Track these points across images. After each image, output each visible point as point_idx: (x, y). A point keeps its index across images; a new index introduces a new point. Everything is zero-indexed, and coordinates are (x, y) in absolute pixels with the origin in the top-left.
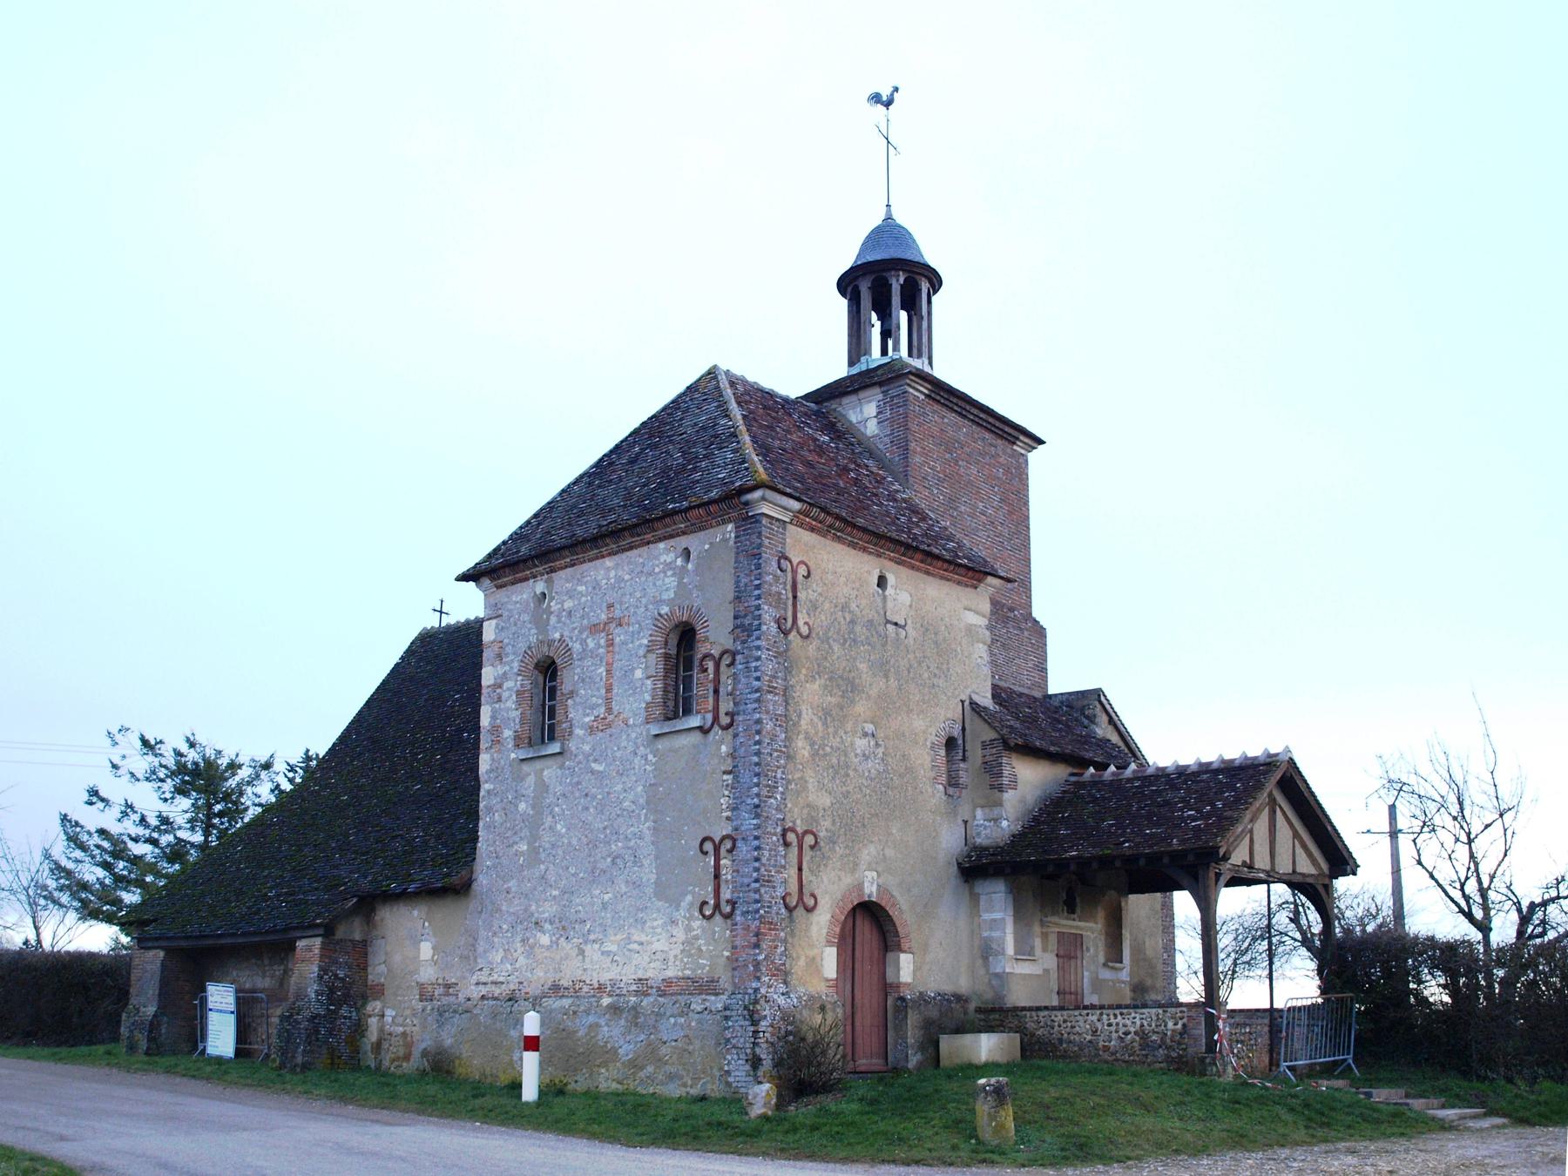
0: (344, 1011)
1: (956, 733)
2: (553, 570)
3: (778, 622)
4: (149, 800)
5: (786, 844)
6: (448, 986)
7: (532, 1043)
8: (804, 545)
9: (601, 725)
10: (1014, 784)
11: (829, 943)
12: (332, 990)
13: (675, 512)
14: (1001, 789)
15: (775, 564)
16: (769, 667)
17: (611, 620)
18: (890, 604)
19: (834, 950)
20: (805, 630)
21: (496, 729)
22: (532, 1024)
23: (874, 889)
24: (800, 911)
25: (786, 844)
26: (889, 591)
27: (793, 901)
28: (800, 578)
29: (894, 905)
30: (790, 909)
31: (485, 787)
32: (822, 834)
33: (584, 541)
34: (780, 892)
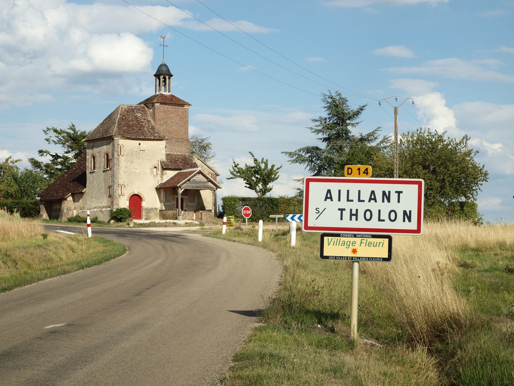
0: (70, 212)
1: (157, 166)
2: (94, 142)
3: (118, 155)
4: (60, 150)
5: (119, 187)
6: (83, 207)
7: (88, 215)
8: (122, 142)
9: (99, 168)
10: (166, 174)
11: (127, 200)
12: (67, 208)
13: (104, 137)
14: (163, 175)
15: (117, 146)
16: (116, 162)
17: (100, 151)
18: (141, 148)
19: (128, 201)
20: (122, 155)
21: (88, 166)
22: (88, 213)
23: (137, 192)
24: (121, 196)
25: (119, 187)
26: (141, 145)
27: (120, 195)
28: (121, 147)
29: (141, 194)
30: (119, 196)
31: (87, 176)
32: (125, 185)
33: (97, 139)
34: (117, 194)
